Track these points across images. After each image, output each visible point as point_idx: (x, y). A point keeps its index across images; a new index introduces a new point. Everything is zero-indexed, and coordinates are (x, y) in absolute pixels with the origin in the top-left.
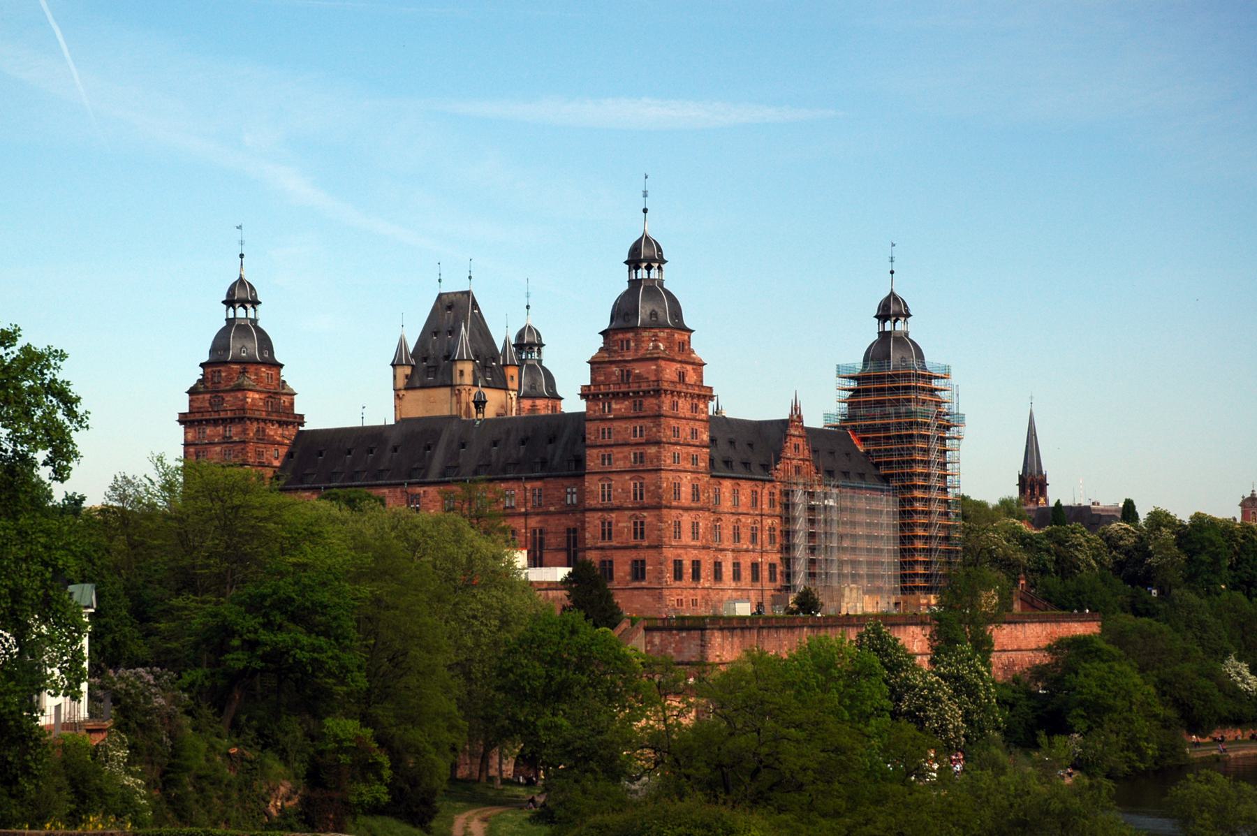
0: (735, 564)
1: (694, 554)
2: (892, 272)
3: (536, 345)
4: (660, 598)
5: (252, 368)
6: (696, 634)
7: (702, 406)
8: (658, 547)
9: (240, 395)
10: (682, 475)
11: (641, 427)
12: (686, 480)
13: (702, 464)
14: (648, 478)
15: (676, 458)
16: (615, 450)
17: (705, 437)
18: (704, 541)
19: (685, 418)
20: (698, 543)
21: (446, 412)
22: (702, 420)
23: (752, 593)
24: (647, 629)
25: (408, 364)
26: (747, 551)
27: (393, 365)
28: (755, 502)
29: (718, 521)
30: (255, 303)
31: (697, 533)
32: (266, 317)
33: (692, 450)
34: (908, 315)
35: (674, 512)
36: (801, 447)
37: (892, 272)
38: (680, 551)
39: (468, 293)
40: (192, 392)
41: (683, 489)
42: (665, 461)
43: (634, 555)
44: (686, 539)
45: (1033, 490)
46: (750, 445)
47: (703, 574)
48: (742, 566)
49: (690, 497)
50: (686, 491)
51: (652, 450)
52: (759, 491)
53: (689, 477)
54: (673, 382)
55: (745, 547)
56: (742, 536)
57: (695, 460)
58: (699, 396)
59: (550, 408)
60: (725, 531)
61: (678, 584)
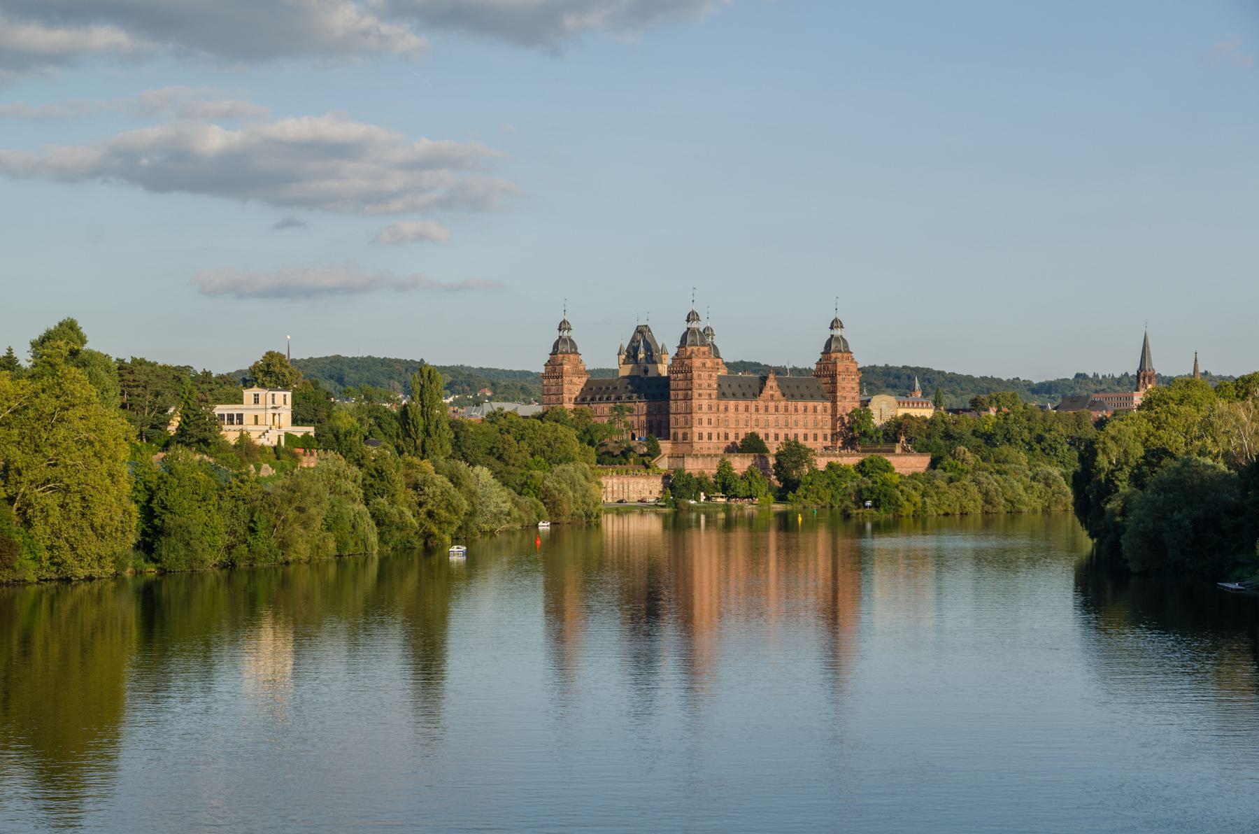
1: (709, 430)
4: (692, 446)
5: (566, 355)
6: (682, 459)
8: (691, 428)
9: (561, 366)
12: (705, 403)
14: (689, 402)
15: (700, 395)
16: (679, 392)
17: (715, 386)
21: (636, 374)
24: (668, 457)
25: (623, 354)
27: (618, 355)
30: (570, 329)
32: (573, 335)
33: (708, 392)
34: (842, 327)
35: (698, 415)
36: (774, 387)
38: (702, 429)
39: (646, 326)
40: (546, 365)
41: (703, 406)
43: (684, 430)
45: (1144, 380)
46: (750, 386)
47: (713, 438)
50: (705, 407)
51: (690, 392)
52: (749, 405)
54: (699, 367)
56: (740, 422)
57: (710, 395)
61: (700, 441)
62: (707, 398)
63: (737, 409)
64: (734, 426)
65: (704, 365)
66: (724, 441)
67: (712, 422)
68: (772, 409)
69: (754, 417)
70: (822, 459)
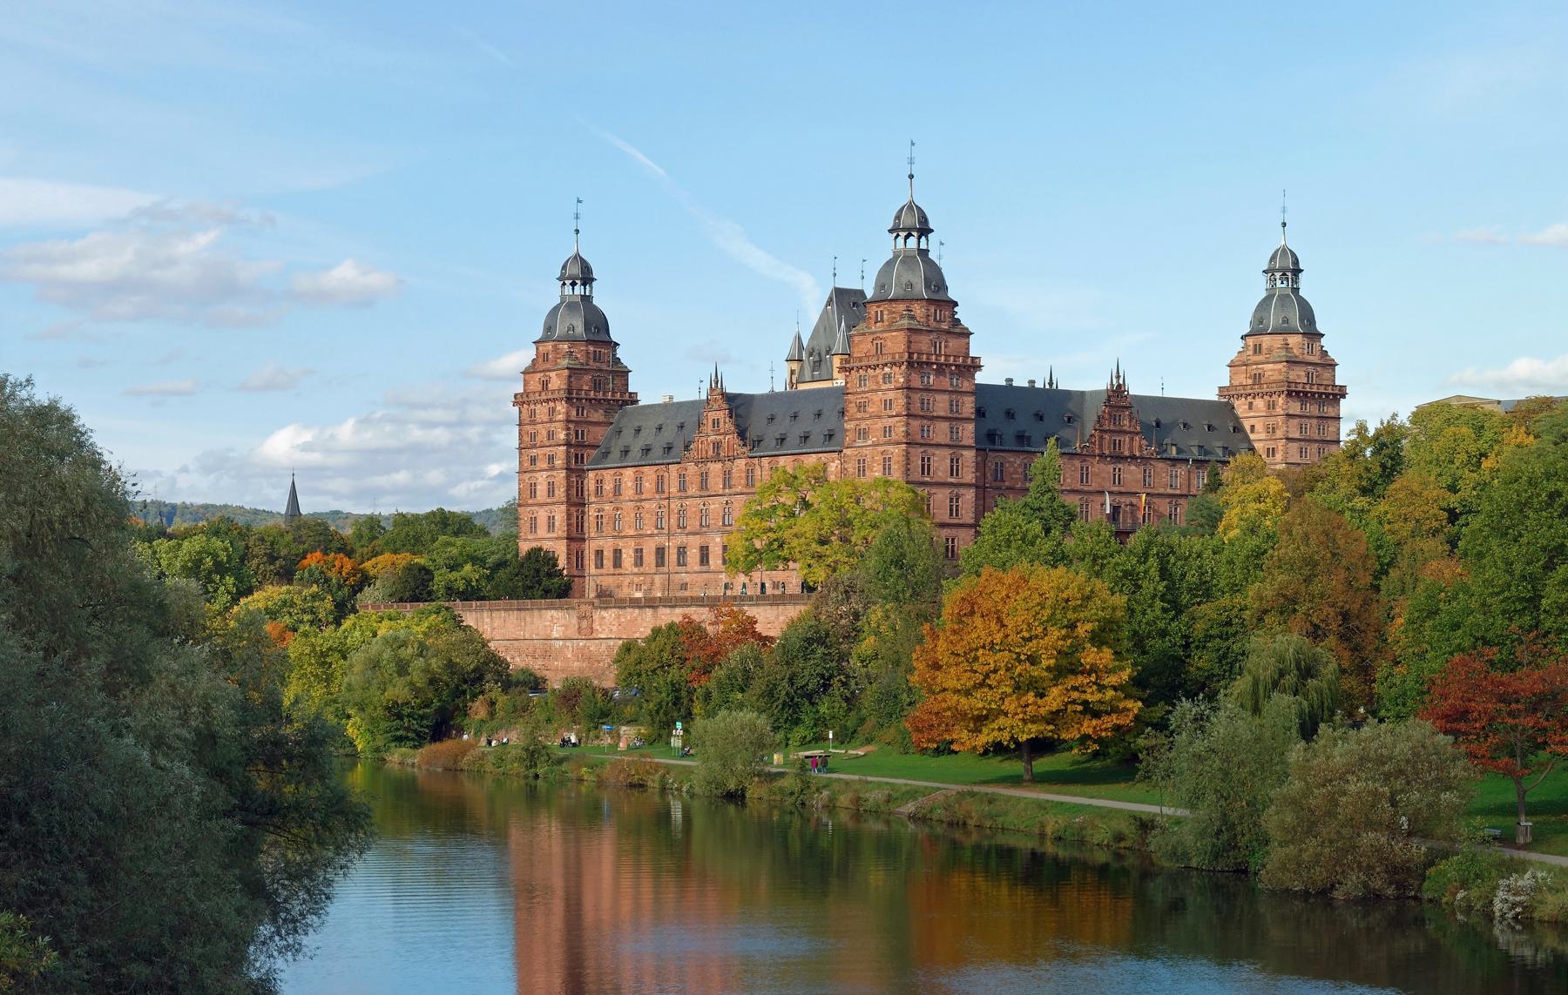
0: (636, 551)
2: (911, 177)
3: (1289, 270)
7: (559, 408)
10: (538, 475)
11: (583, 432)
13: (560, 462)
17: (562, 436)
18: (560, 532)
19: (542, 423)
20: (555, 535)
22: (560, 421)
23: (657, 578)
26: (651, 535)
28: (659, 489)
29: (618, 509)
31: (553, 526)
36: (721, 424)
37: (911, 177)
41: (538, 487)
42: (523, 465)
44: (542, 531)
48: (644, 551)
49: (546, 493)
52: (666, 474)
53: (544, 476)
55: (649, 532)
58: (554, 400)
59: (1251, 347)
60: (627, 519)
62: (545, 466)
63: (639, 489)
64: (632, 532)
65: (545, 384)
66: (612, 571)
67: (557, 524)
68: (716, 483)
69: (676, 504)
70: (604, 613)
